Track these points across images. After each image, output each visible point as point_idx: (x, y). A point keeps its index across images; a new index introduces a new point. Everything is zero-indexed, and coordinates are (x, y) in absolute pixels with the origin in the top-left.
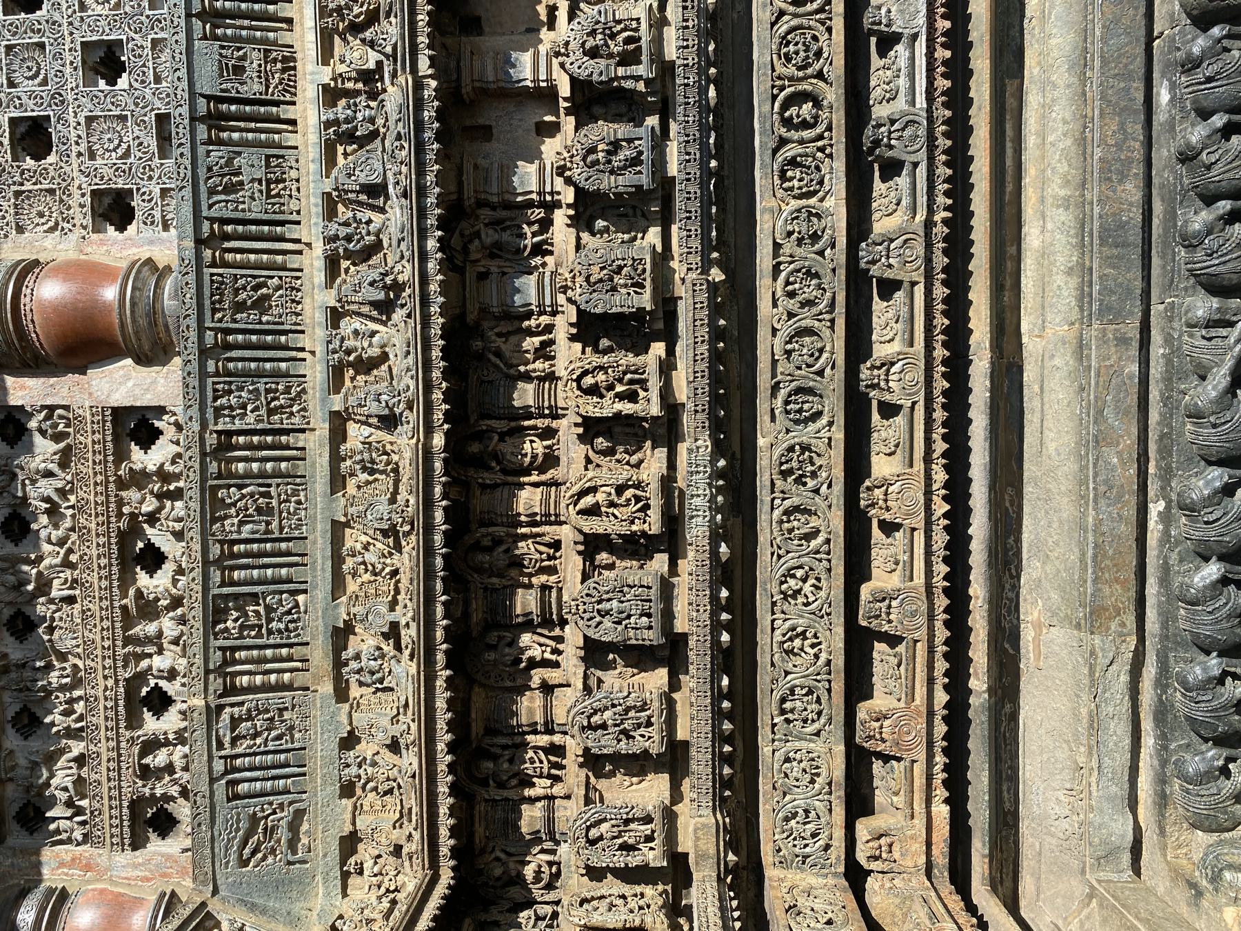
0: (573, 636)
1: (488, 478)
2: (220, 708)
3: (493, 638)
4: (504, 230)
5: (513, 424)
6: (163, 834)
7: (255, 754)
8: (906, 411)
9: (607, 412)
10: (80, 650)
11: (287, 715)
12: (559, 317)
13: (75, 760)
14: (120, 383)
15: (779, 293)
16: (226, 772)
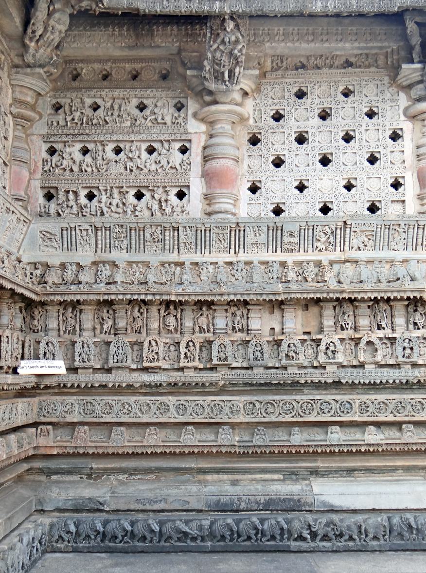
0: (111, 338)
1: (162, 312)
2: (91, 226)
3: (111, 312)
4: (240, 317)
5: (179, 319)
6: (44, 196)
7: (76, 236)
8: (178, 440)
9: (181, 349)
10: (109, 171)
11: (88, 246)
12: (212, 334)
13: (71, 169)
14: (197, 188)
15: (216, 402)
16: (70, 227)
